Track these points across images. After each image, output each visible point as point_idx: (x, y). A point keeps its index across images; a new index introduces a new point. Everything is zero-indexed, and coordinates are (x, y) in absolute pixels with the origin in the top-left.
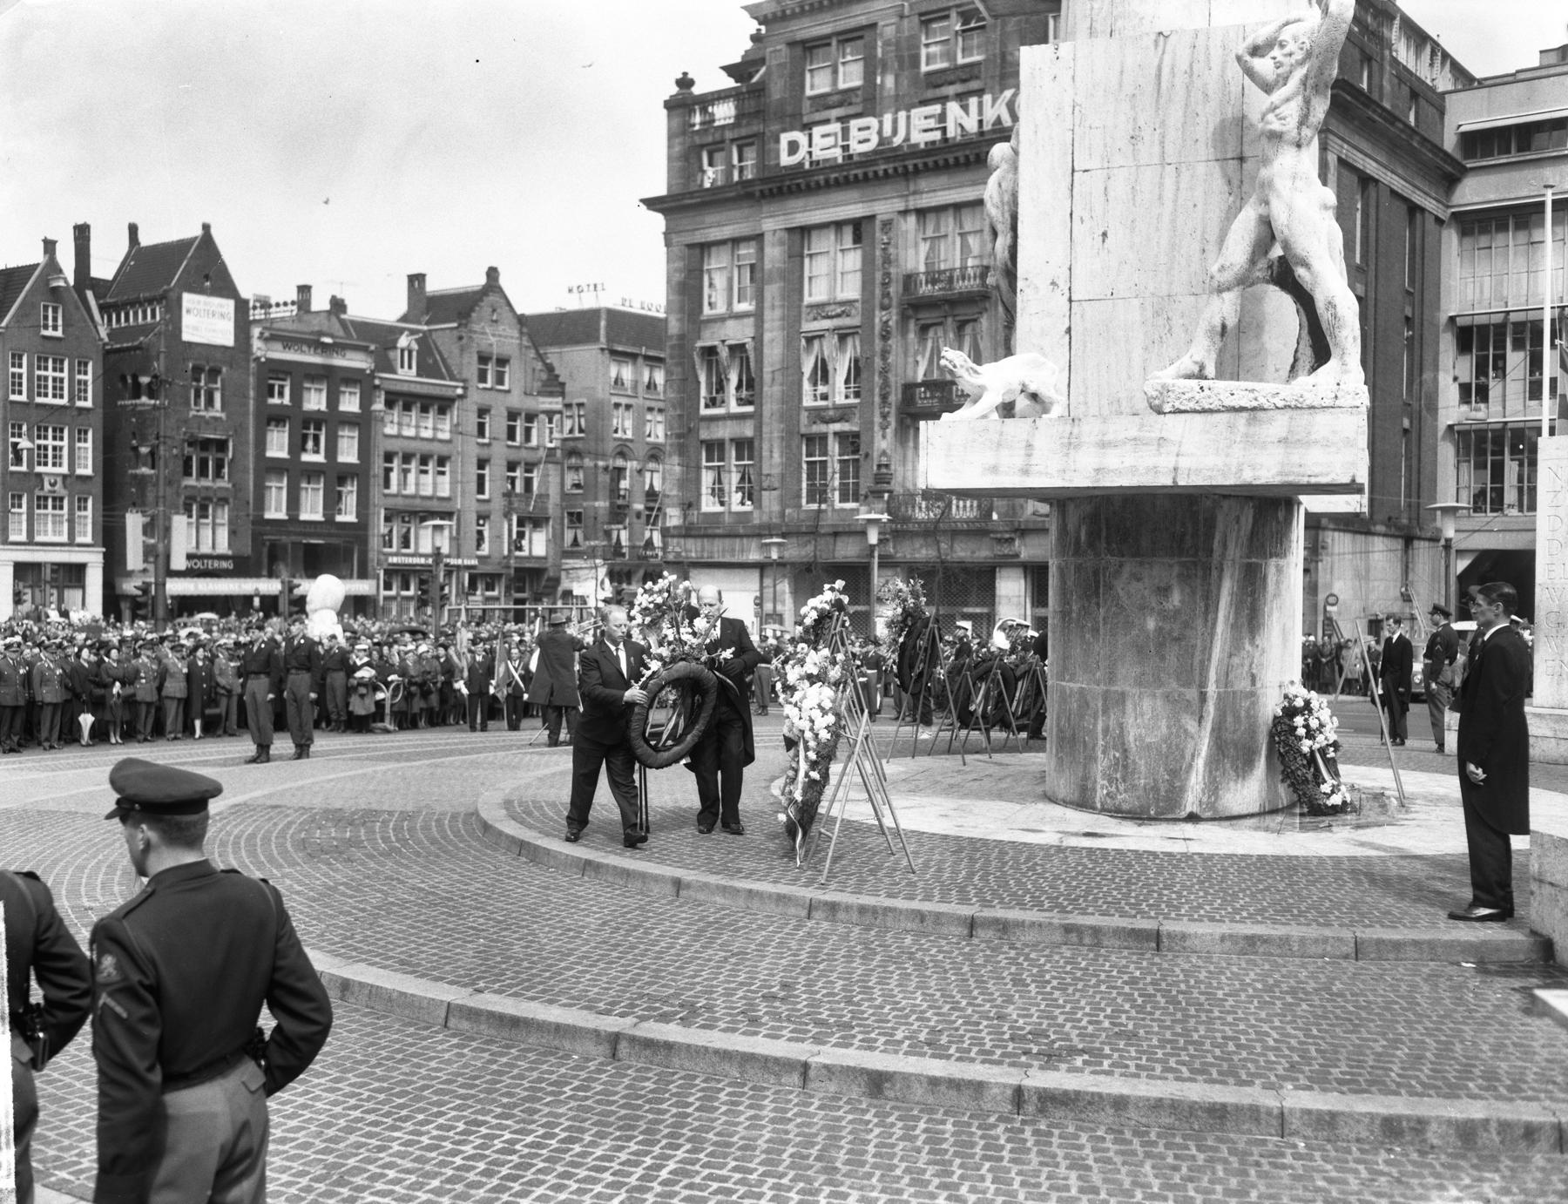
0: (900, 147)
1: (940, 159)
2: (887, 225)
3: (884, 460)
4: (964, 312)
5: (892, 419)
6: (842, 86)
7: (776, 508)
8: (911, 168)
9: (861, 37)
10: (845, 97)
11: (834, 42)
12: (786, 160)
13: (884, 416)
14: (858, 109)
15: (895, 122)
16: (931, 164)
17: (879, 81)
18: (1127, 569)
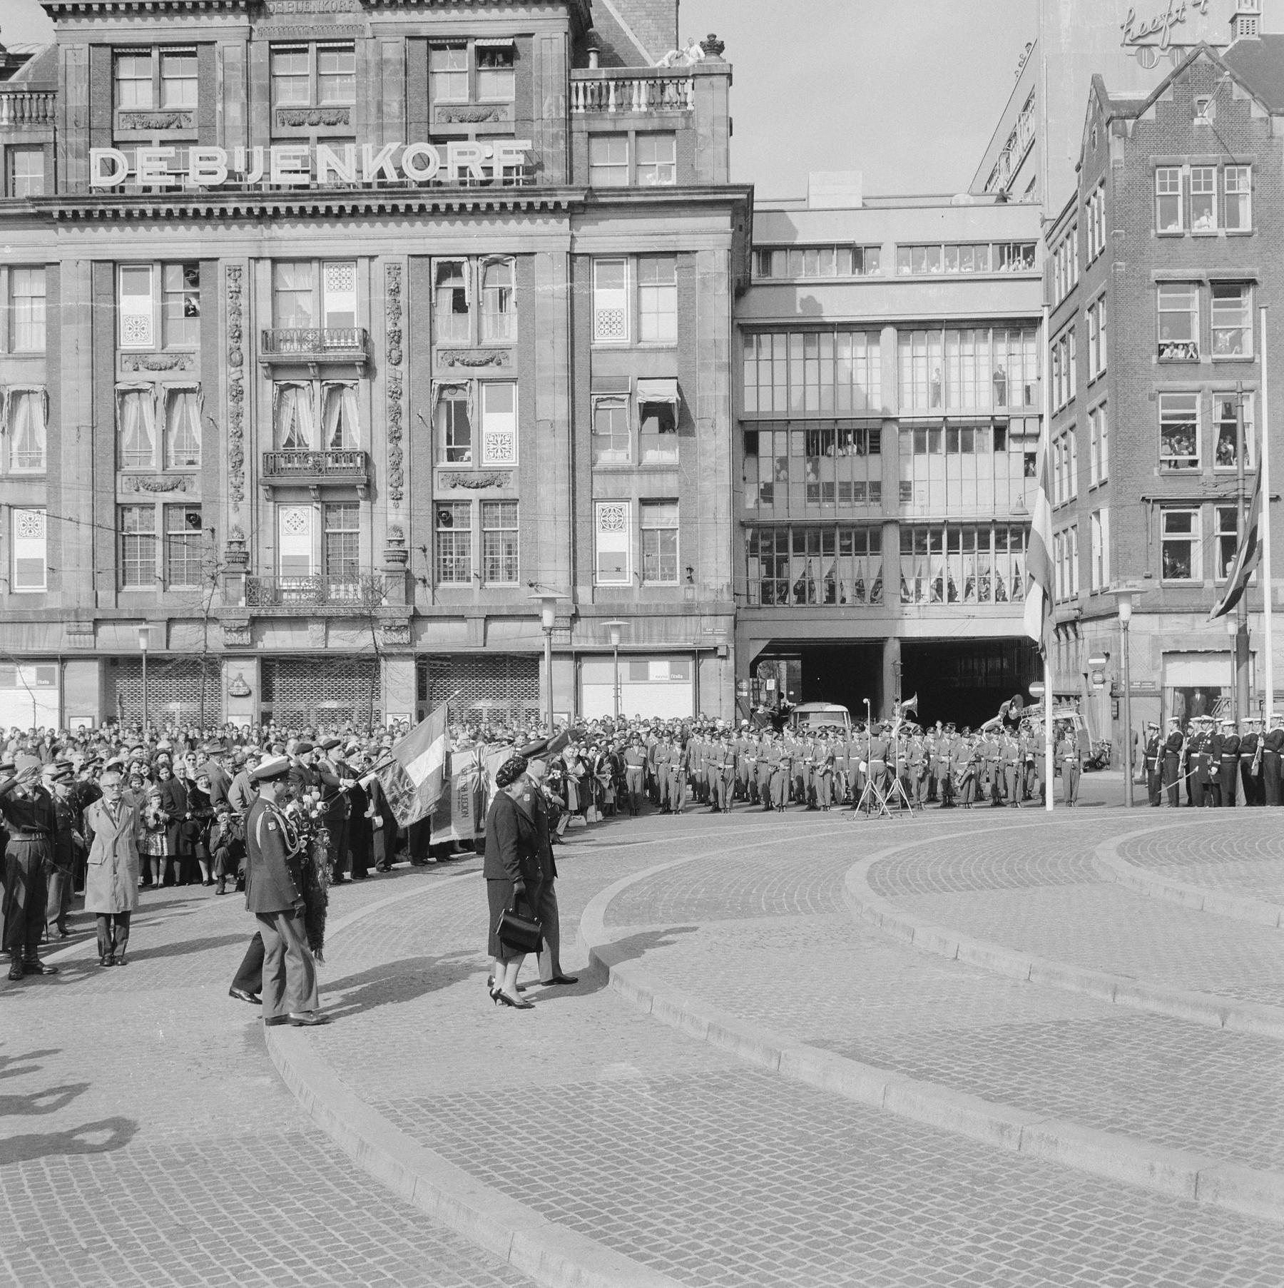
0: (258, 187)
1: (309, 206)
2: (235, 271)
3: (236, 537)
4: (335, 378)
5: (246, 490)
6: (169, 106)
7: (86, 589)
8: (270, 211)
9: (193, 54)
10: (175, 118)
11: (155, 53)
12: (100, 181)
13: (237, 488)
14: (194, 135)
15: (249, 156)
16: (296, 210)
17: (219, 107)
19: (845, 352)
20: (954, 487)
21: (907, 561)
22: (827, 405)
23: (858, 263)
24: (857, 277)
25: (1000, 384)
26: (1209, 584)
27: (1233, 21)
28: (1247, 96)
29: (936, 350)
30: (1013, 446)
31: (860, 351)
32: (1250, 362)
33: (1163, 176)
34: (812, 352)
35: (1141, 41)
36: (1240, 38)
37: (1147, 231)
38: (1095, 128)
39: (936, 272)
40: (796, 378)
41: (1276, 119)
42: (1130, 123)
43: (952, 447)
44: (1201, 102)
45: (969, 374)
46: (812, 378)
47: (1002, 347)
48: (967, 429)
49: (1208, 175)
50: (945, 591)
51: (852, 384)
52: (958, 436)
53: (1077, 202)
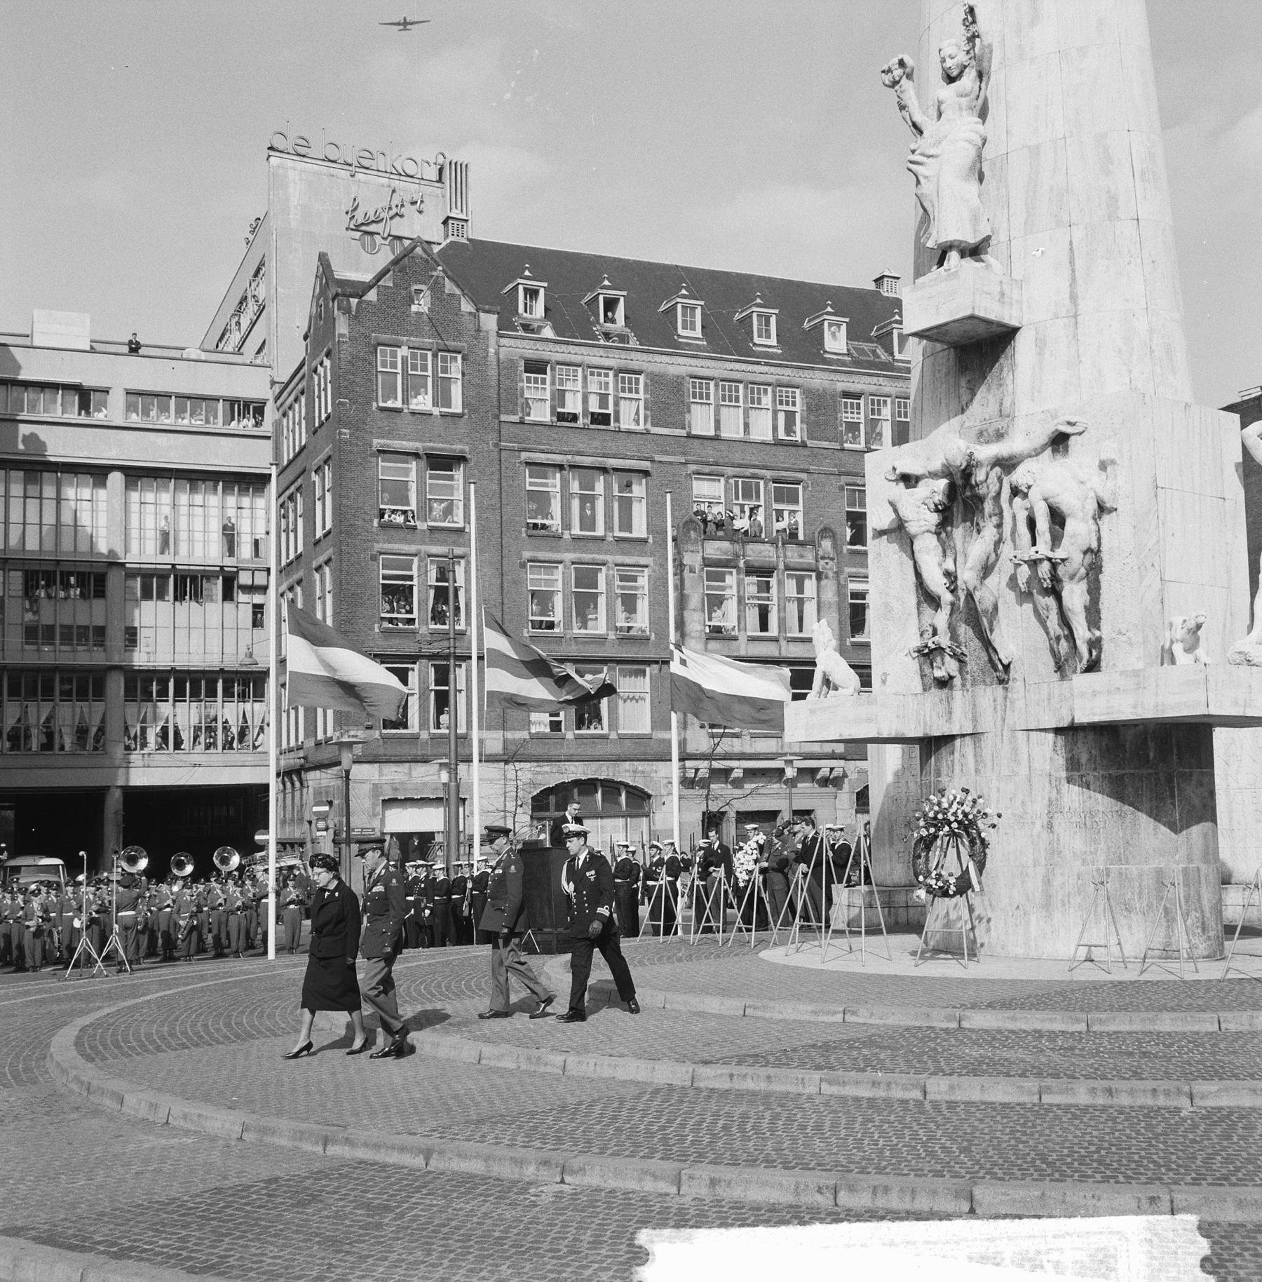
18: (1194, 778)
19: (69, 492)
20: (181, 634)
21: (131, 708)
22: (49, 545)
23: (85, 406)
24: (83, 419)
25: (230, 536)
26: (424, 735)
27: (445, 222)
28: (458, 292)
29: (166, 497)
30: (242, 597)
31: (86, 493)
32: (461, 531)
33: (384, 354)
34: (33, 490)
35: (363, 228)
36: (451, 239)
37: (369, 403)
38: (321, 302)
39: (168, 421)
40: (15, 516)
41: (482, 315)
42: (354, 301)
43: (179, 597)
44: (418, 291)
45: (198, 524)
46: (32, 517)
47: (231, 500)
48: (194, 578)
49: (424, 358)
50: (171, 739)
51: (76, 526)
52: (188, 584)
53: (306, 367)
